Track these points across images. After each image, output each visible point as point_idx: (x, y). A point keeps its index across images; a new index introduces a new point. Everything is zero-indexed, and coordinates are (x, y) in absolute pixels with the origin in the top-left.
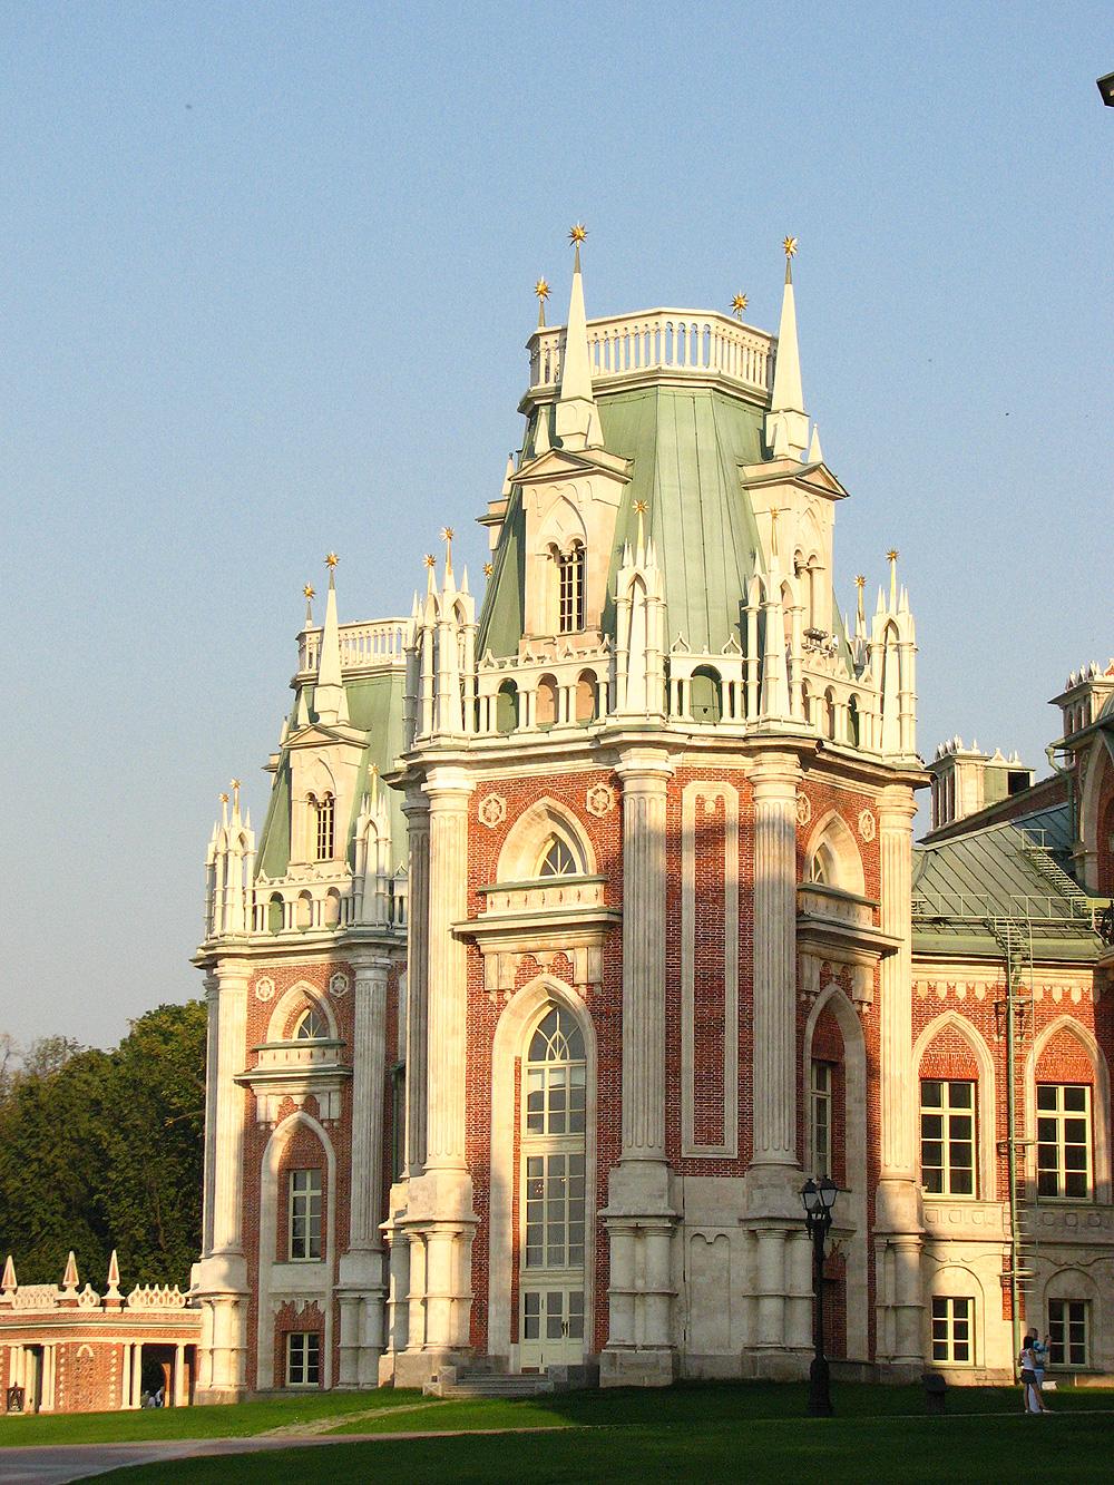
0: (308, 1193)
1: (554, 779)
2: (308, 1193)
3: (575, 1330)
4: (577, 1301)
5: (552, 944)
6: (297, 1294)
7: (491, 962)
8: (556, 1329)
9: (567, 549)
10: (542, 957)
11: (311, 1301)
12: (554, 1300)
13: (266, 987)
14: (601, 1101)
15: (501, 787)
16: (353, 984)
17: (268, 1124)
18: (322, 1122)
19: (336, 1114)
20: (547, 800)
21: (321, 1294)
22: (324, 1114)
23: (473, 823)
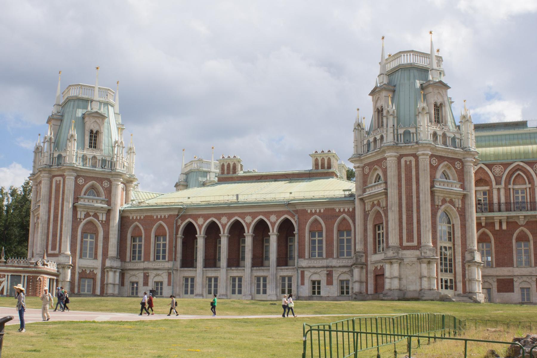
0: (89, 240)
1: (448, 158)
2: (162, 242)
3: (451, 288)
4: (451, 280)
5: (451, 196)
6: (88, 268)
7: (436, 197)
8: (446, 288)
9: (438, 104)
10: (448, 199)
11: (92, 270)
12: (446, 282)
13: (81, 181)
14: (462, 235)
15: (436, 157)
16: (111, 186)
17: (80, 219)
18: (99, 221)
19: (104, 219)
20: (446, 163)
21: (96, 268)
22: (100, 219)
23: (431, 164)
